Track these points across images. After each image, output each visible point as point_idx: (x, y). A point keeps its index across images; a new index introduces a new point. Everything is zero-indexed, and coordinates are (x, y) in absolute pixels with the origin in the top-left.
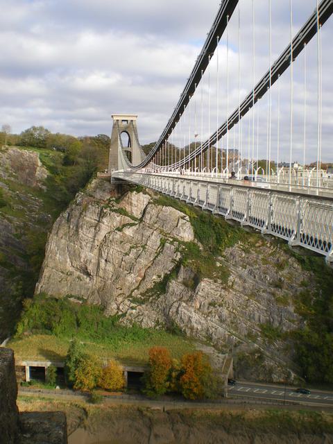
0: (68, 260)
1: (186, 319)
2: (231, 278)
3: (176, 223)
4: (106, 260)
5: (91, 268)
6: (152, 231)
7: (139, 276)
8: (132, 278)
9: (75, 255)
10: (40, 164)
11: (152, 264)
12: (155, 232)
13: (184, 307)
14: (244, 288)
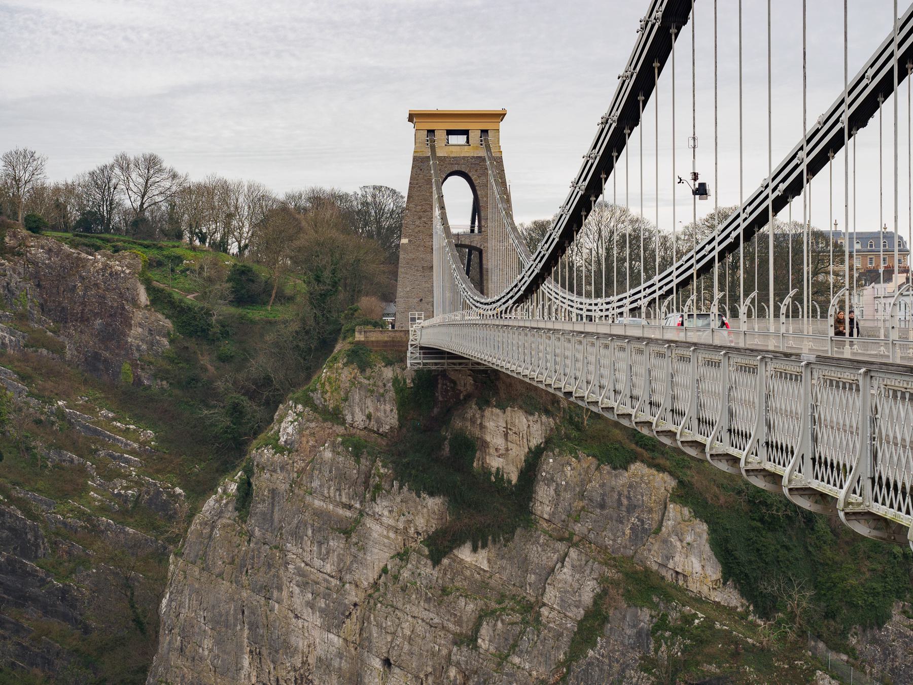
0: (246, 661)
3: (656, 517)
4: (387, 663)
6: (561, 546)
10: (143, 298)
12: (573, 553)
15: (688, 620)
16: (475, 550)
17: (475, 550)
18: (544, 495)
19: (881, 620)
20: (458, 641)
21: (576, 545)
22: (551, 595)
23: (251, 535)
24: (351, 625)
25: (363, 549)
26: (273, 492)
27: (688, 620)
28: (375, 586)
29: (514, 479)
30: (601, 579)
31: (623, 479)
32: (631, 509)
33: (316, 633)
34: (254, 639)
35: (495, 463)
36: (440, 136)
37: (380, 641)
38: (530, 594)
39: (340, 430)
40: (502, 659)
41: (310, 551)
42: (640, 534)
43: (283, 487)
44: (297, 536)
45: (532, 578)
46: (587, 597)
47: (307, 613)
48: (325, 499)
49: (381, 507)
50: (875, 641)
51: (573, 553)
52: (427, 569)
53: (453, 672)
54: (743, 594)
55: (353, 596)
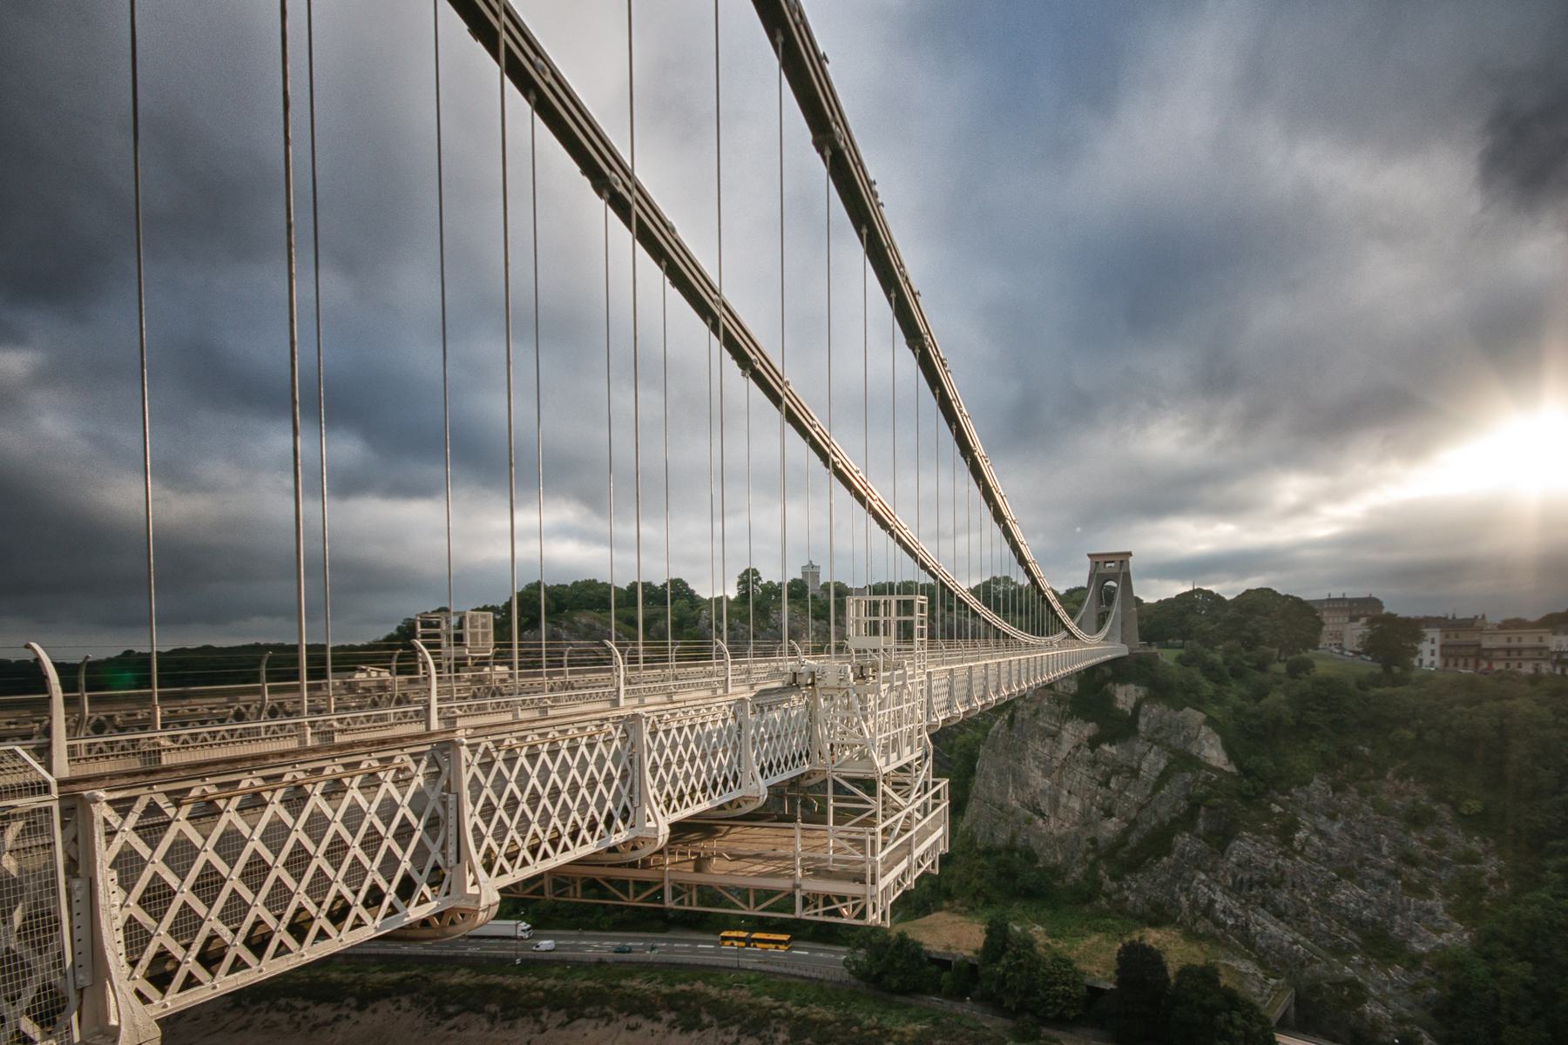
1: (1203, 901)
2: (1300, 835)
4: (1069, 792)
5: (1044, 805)
6: (1150, 744)
7: (1126, 821)
8: (1112, 826)
9: (1021, 782)
11: (1150, 802)
12: (1155, 748)
13: (1202, 882)
14: (1329, 856)
15: (1209, 778)
16: (1110, 746)
17: (1110, 746)
18: (1142, 721)
19: (1307, 783)
20: (1100, 784)
21: (1157, 744)
22: (1145, 766)
23: (1014, 737)
24: (1055, 776)
25: (1060, 744)
26: (1023, 720)
27: (1209, 778)
28: (1065, 759)
29: (1130, 713)
30: (1169, 758)
31: (1181, 714)
32: (1183, 728)
33: (1040, 779)
34: (1014, 780)
35: (1121, 706)
36: (1101, 564)
37: (1067, 783)
38: (1135, 765)
39: (1052, 692)
40: (1120, 792)
41: (1038, 745)
42: (1188, 740)
43: (1027, 717)
44: (1032, 737)
45: (1136, 758)
46: (1161, 766)
47: (1036, 770)
48: (1044, 722)
49: (1068, 726)
50: (1303, 791)
51: (1155, 748)
52: (1088, 753)
53: (1098, 798)
54: (1237, 766)
55: (1056, 763)
